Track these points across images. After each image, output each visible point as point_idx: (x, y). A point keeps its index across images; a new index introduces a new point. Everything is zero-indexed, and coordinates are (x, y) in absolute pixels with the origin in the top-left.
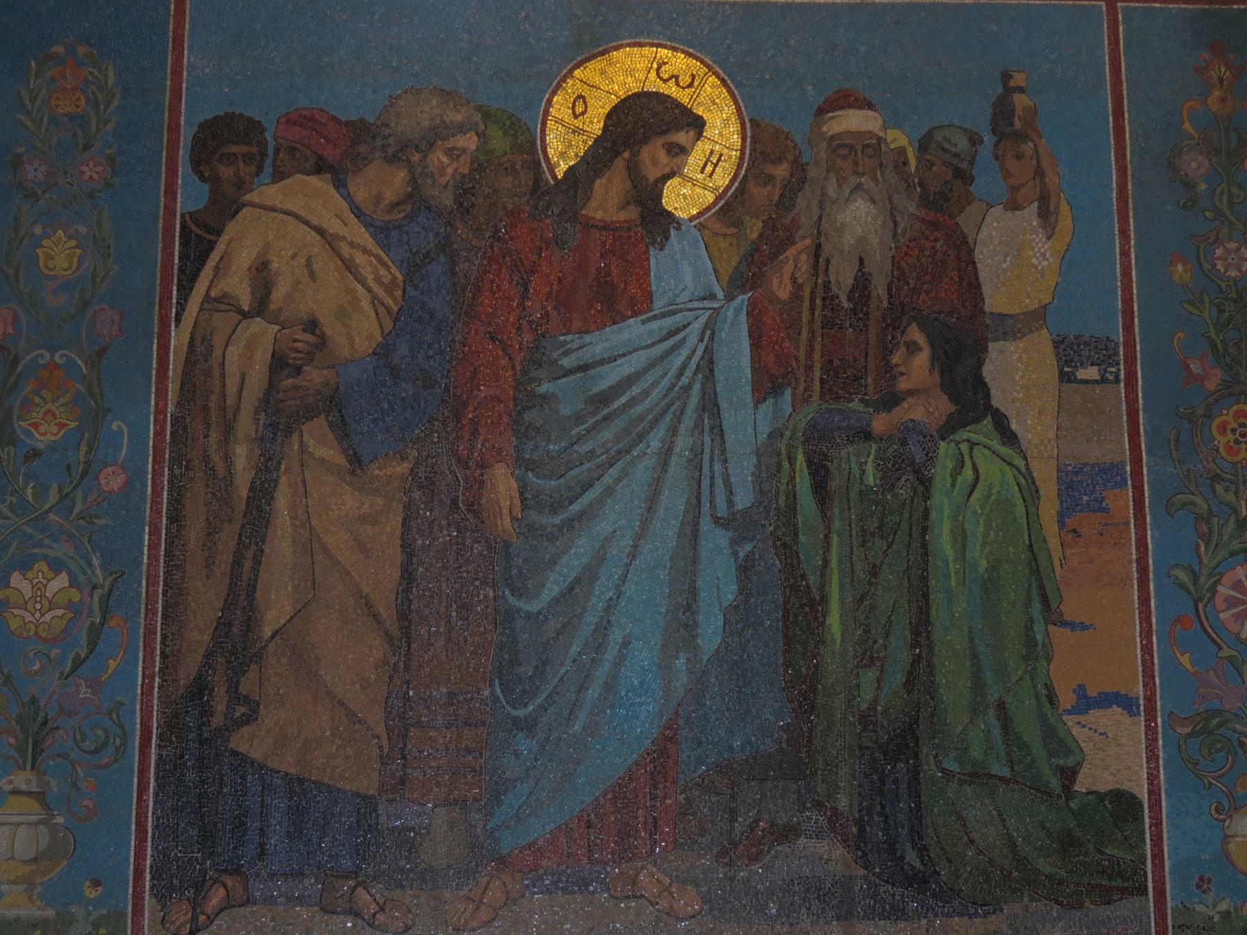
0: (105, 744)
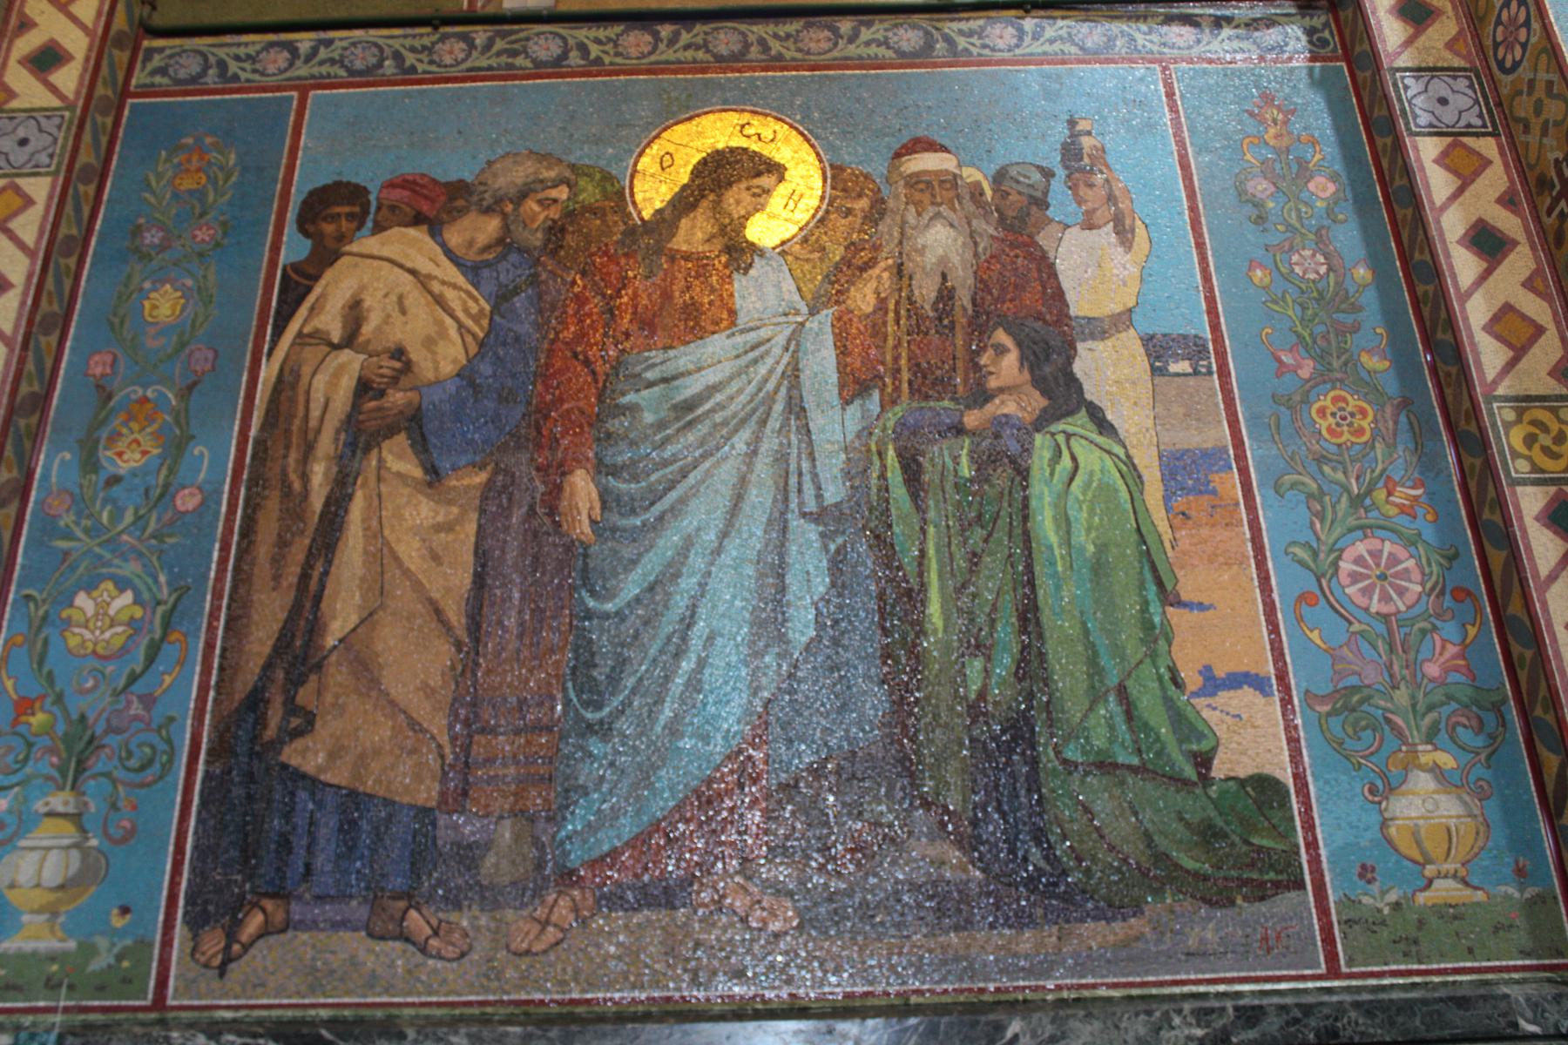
0: (150, 762)
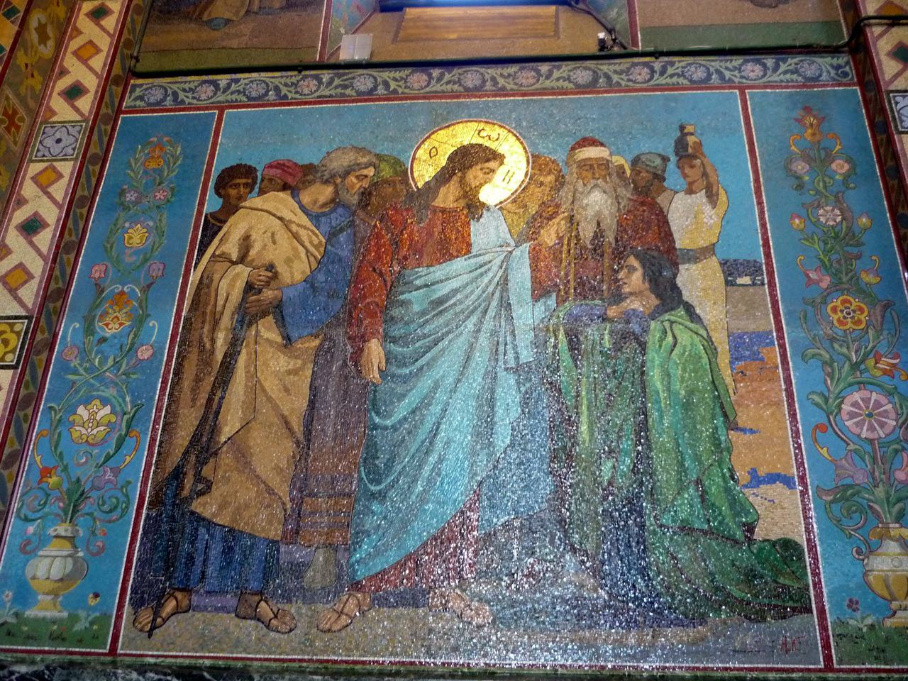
0: (116, 507)
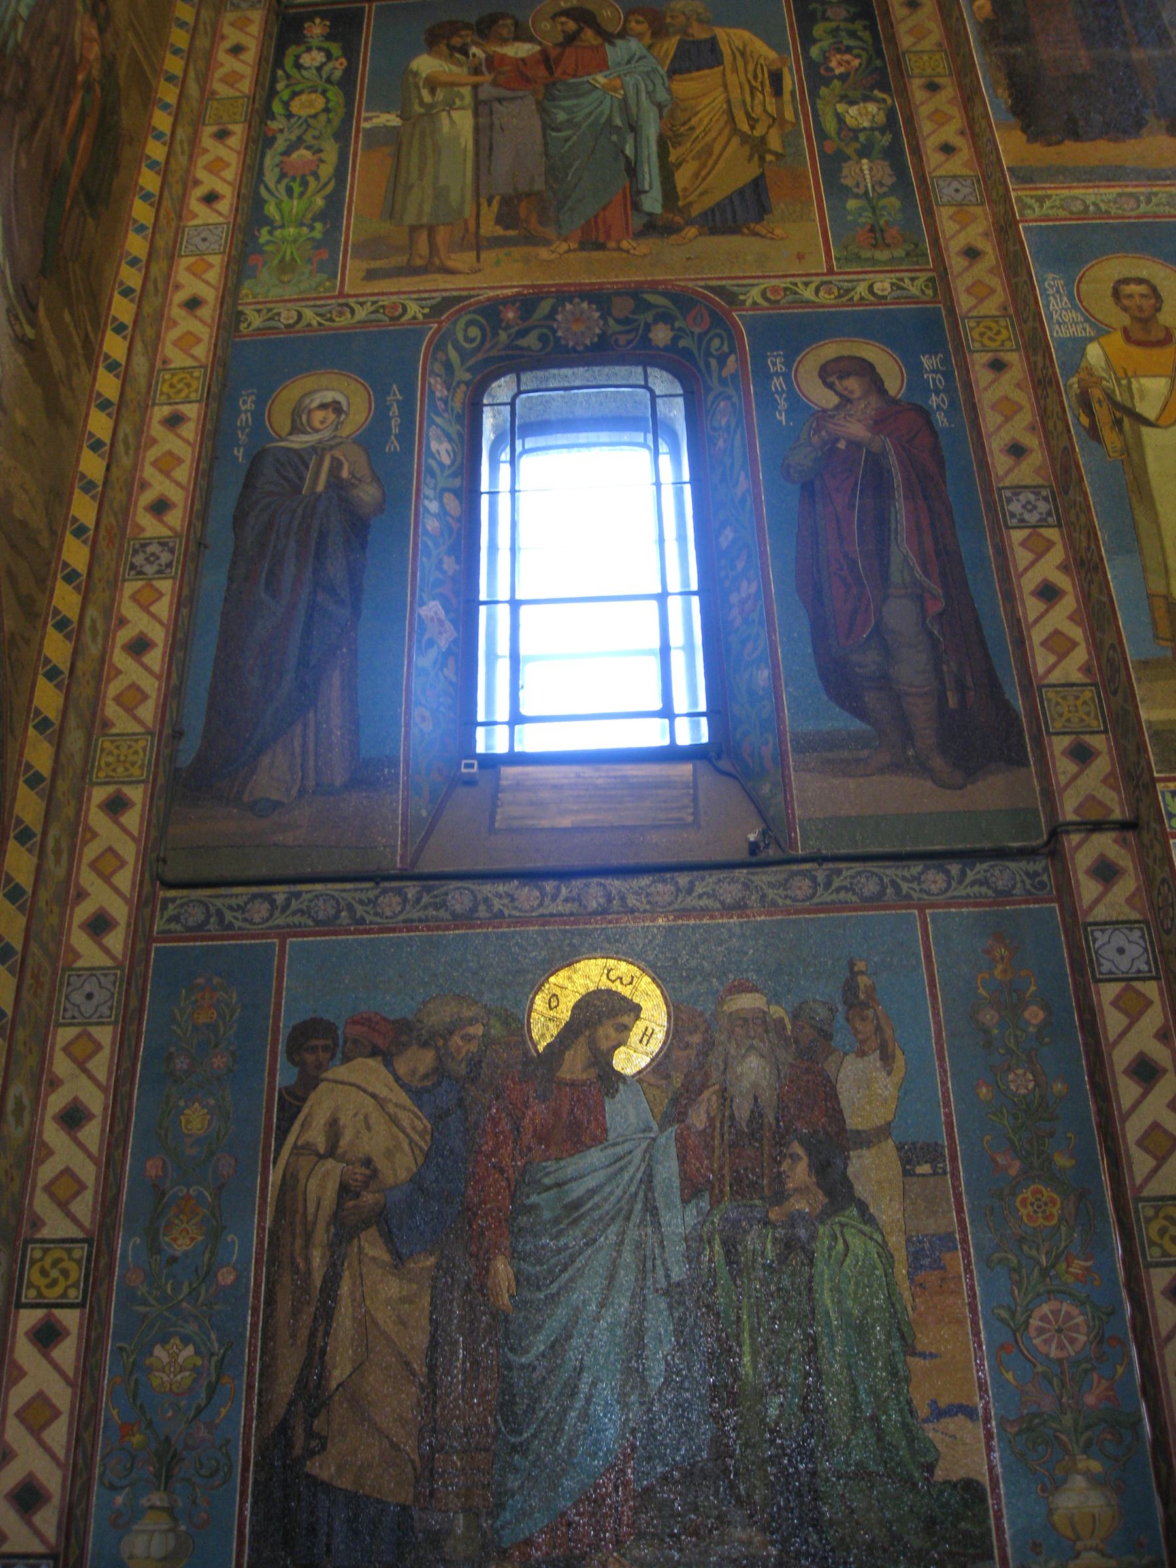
0: (217, 1471)
